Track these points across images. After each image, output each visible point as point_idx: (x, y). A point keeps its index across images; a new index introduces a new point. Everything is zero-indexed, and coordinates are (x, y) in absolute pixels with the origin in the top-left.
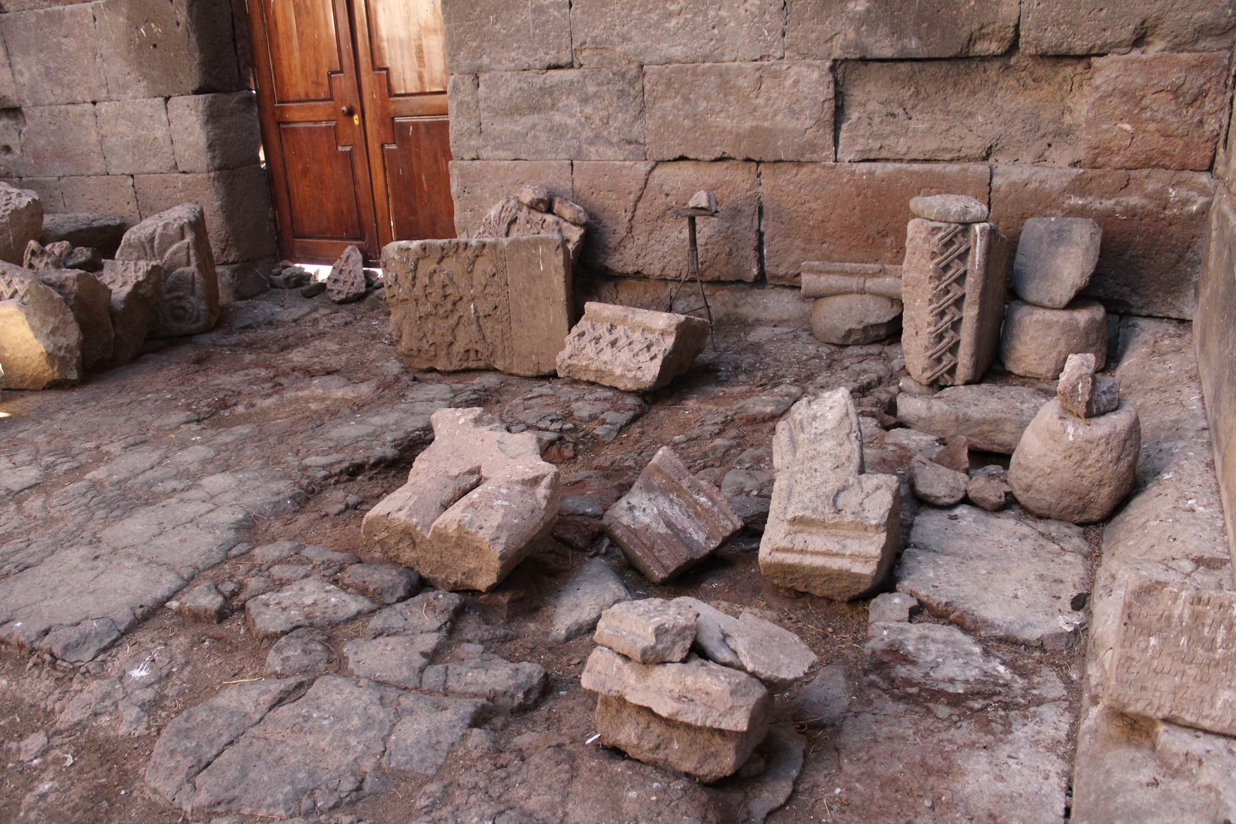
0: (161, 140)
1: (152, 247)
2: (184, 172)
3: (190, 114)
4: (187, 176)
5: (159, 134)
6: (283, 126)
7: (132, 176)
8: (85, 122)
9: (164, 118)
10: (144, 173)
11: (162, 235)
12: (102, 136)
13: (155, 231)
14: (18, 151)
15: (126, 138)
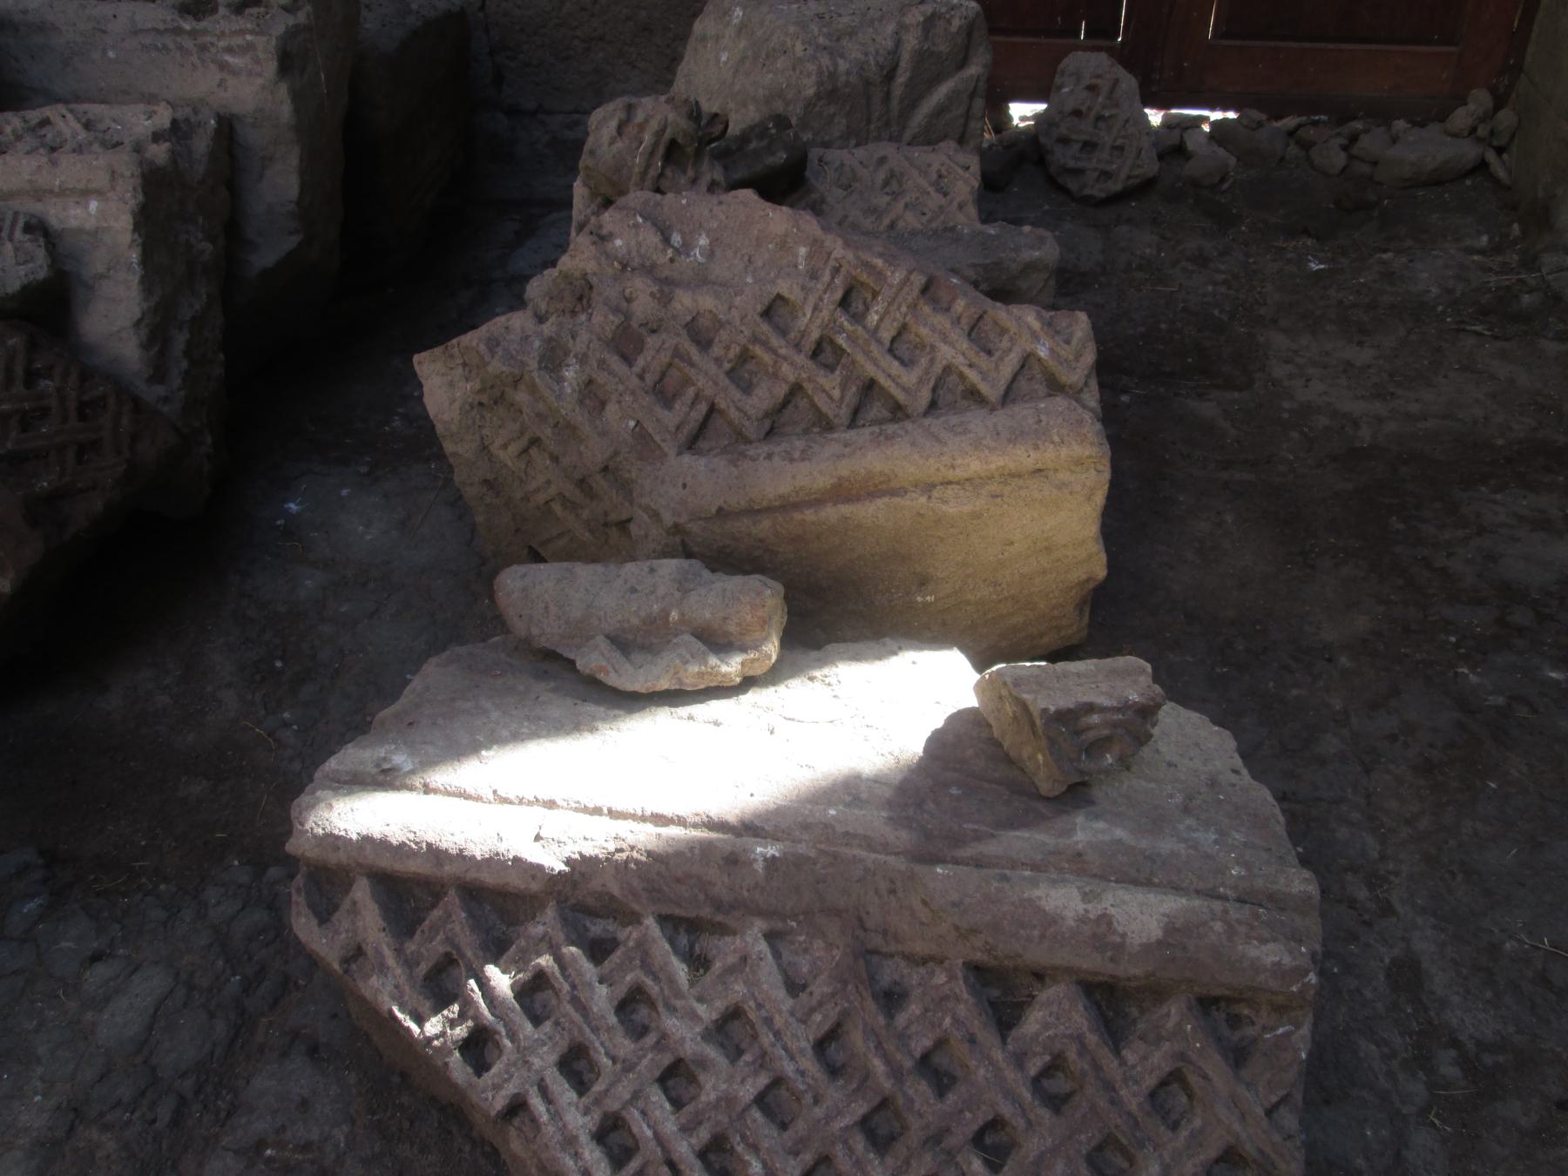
1: (887, 97)
11: (921, 57)
13: (898, 43)
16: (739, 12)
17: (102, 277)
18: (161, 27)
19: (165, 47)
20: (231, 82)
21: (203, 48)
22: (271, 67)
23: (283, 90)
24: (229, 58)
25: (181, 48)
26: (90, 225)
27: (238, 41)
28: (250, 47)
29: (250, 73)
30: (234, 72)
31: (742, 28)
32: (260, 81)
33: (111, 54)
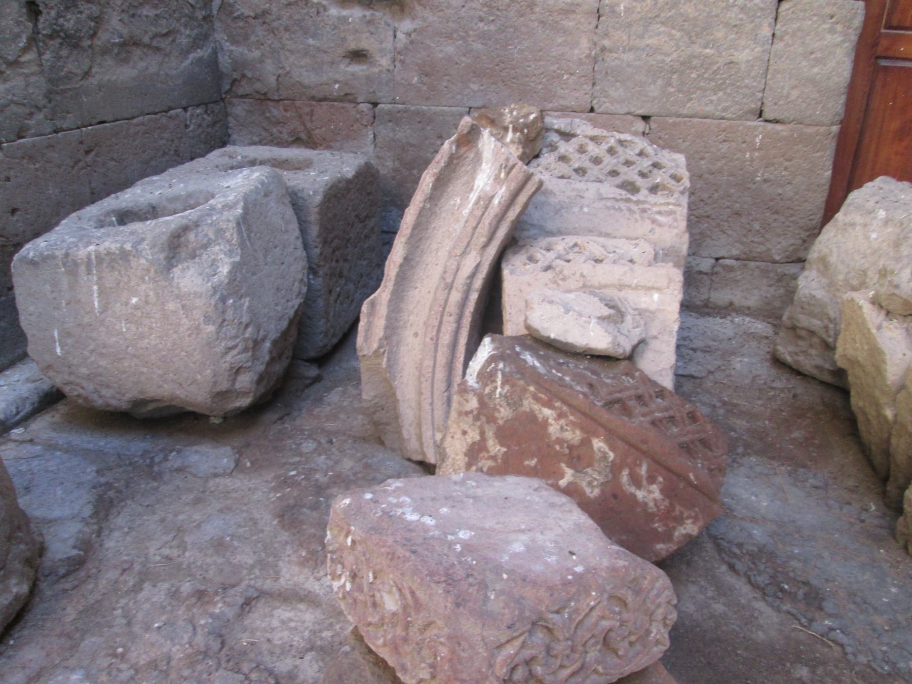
0: (743, 67)
2: (766, 121)
3: (832, 31)
4: (779, 127)
5: (743, 56)
6: (884, 63)
7: (646, 118)
8: (569, 24)
9: (766, 32)
10: (679, 116)
12: (603, 49)
14: (385, 62)
15: (660, 57)
16: (882, 214)
17: (655, 337)
18: (619, 197)
19: (620, 209)
20: (658, 230)
21: (644, 211)
22: (683, 224)
23: (686, 237)
24: (658, 217)
25: (629, 210)
26: (653, 307)
27: (663, 208)
28: (670, 213)
29: (670, 227)
30: (660, 225)
31: (887, 222)
32: (676, 231)
33: (586, 210)
